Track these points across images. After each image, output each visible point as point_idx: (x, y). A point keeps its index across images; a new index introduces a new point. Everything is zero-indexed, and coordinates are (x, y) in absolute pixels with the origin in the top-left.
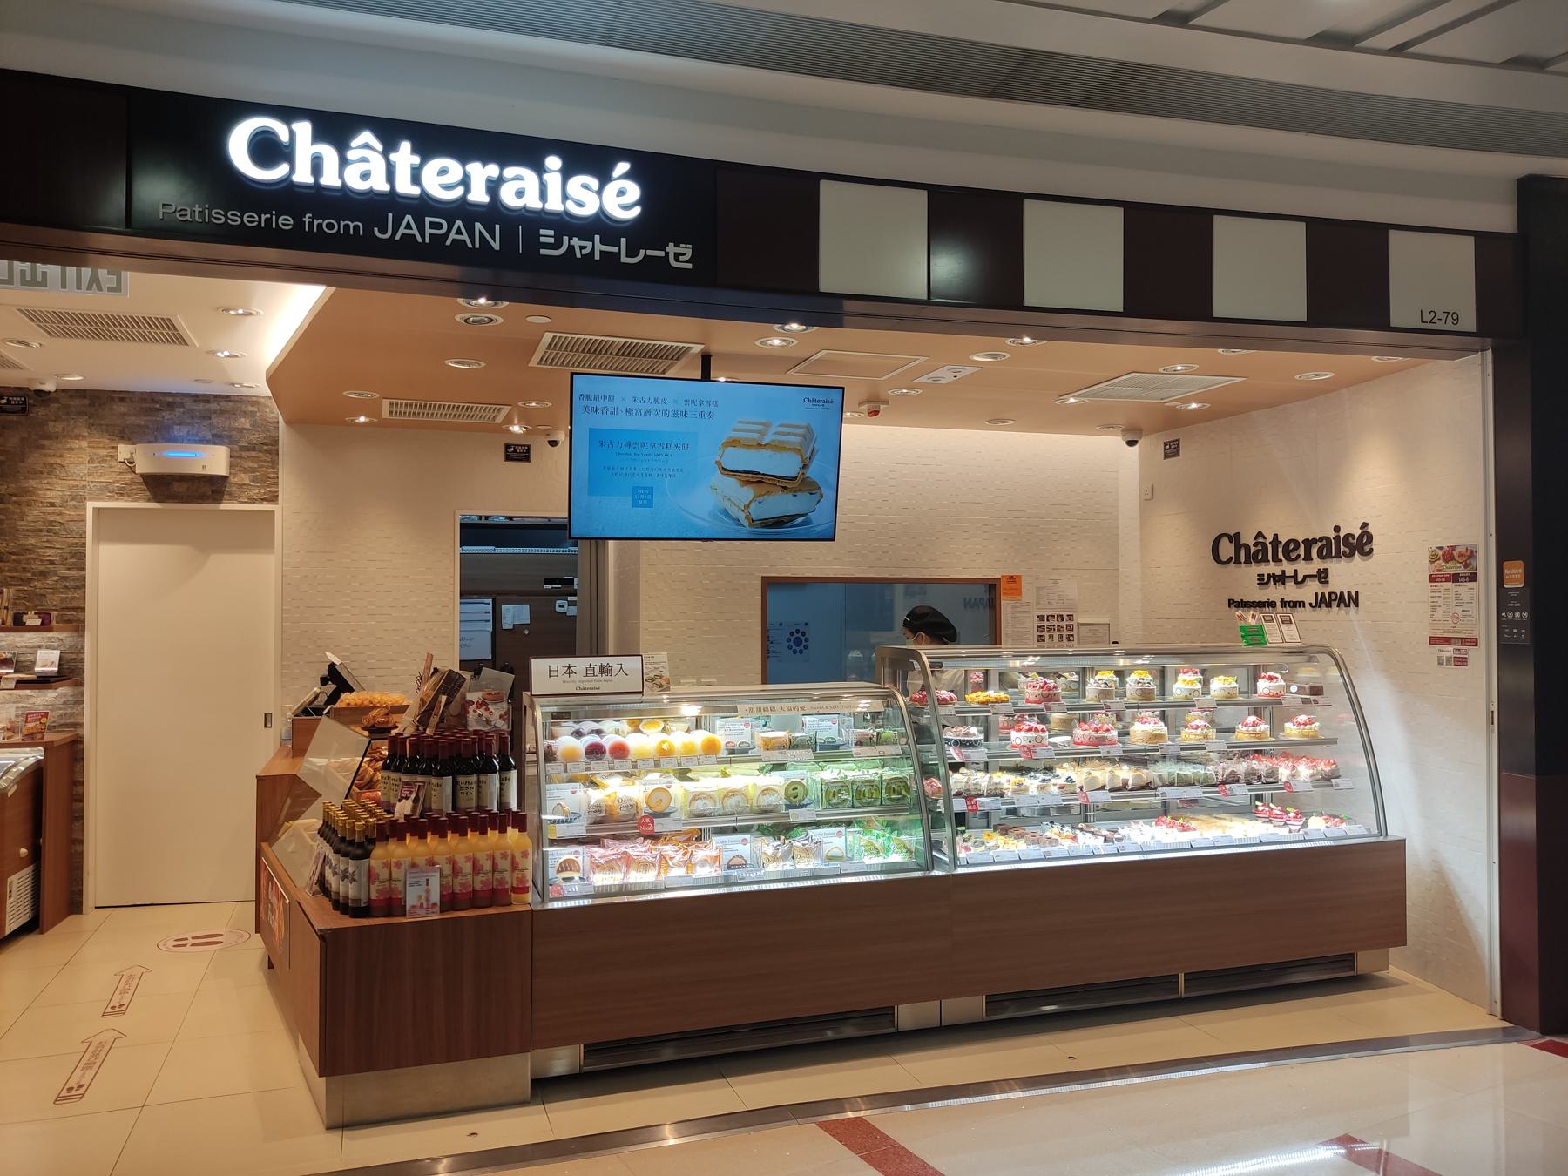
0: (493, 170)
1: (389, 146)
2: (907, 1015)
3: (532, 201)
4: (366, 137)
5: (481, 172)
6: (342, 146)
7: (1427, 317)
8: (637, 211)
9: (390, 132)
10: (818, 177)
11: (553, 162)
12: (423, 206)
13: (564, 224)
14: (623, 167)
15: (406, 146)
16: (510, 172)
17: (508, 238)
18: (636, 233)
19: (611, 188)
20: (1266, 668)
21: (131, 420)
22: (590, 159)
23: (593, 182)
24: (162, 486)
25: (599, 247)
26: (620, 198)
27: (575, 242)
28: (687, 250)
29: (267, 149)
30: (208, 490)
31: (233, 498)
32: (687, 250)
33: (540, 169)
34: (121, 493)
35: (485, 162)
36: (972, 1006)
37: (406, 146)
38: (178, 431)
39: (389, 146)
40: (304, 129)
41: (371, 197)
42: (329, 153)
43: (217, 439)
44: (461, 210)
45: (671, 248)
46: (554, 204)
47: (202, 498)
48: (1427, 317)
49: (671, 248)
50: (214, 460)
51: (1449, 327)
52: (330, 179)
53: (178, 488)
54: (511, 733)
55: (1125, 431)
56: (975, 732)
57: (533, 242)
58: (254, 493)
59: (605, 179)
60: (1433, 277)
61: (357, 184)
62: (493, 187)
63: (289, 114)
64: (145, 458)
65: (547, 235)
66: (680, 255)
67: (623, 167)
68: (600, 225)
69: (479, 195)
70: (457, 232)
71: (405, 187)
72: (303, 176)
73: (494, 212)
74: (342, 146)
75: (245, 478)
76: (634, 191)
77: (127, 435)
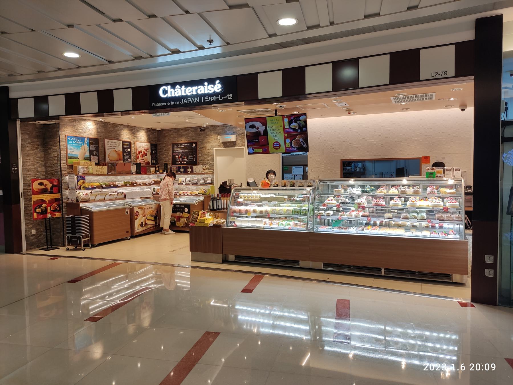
0: (196, 87)
1: (181, 87)
2: (302, 264)
3: (203, 92)
4: (178, 86)
5: (195, 88)
6: (174, 89)
7: (434, 75)
8: (220, 90)
9: (181, 84)
10: (256, 74)
11: (206, 83)
12: (187, 97)
13: (209, 95)
14: (218, 81)
15: (183, 86)
16: (199, 87)
17: (200, 100)
18: (221, 94)
19: (216, 86)
20: (428, 186)
21: (220, 131)
22: (212, 81)
23: (212, 86)
24: (226, 144)
25: (215, 98)
26: (217, 87)
27: (211, 98)
28: (231, 95)
29: (165, 92)
30: (233, 144)
31: (237, 146)
32: (231, 95)
33: (204, 85)
34: (219, 146)
35: (195, 86)
36: (319, 265)
37: (183, 86)
38: (228, 132)
39: (181, 86)
40: (169, 87)
41: (179, 97)
42: (173, 90)
43: (234, 134)
44: (192, 96)
45: (228, 96)
46: (206, 92)
47: (232, 146)
48: (434, 75)
49: (228, 96)
50: (232, 138)
51: (443, 76)
52: (173, 95)
53: (228, 144)
54: (294, 200)
55: (460, 106)
56: (82, 181)
57: (204, 99)
58: (241, 145)
59: (214, 84)
60: (439, 60)
61: (177, 95)
62: (197, 90)
63: (167, 85)
64: (221, 139)
65: (206, 97)
66: (230, 96)
67: (218, 81)
68: (215, 94)
69: (194, 93)
70: (192, 100)
71: (184, 94)
72: (169, 95)
73: (197, 95)
74: (174, 89)
75: (239, 141)
76: (220, 86)
77: (219, 134)
